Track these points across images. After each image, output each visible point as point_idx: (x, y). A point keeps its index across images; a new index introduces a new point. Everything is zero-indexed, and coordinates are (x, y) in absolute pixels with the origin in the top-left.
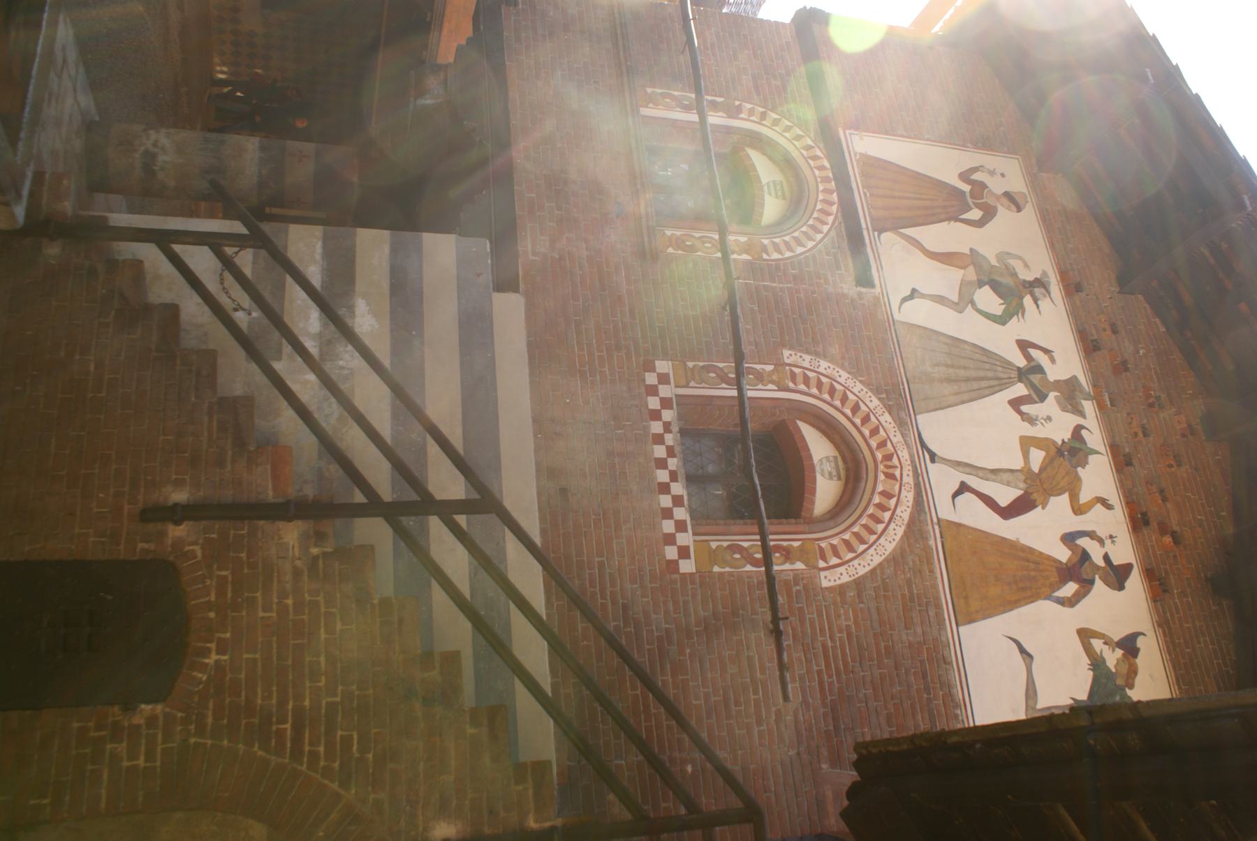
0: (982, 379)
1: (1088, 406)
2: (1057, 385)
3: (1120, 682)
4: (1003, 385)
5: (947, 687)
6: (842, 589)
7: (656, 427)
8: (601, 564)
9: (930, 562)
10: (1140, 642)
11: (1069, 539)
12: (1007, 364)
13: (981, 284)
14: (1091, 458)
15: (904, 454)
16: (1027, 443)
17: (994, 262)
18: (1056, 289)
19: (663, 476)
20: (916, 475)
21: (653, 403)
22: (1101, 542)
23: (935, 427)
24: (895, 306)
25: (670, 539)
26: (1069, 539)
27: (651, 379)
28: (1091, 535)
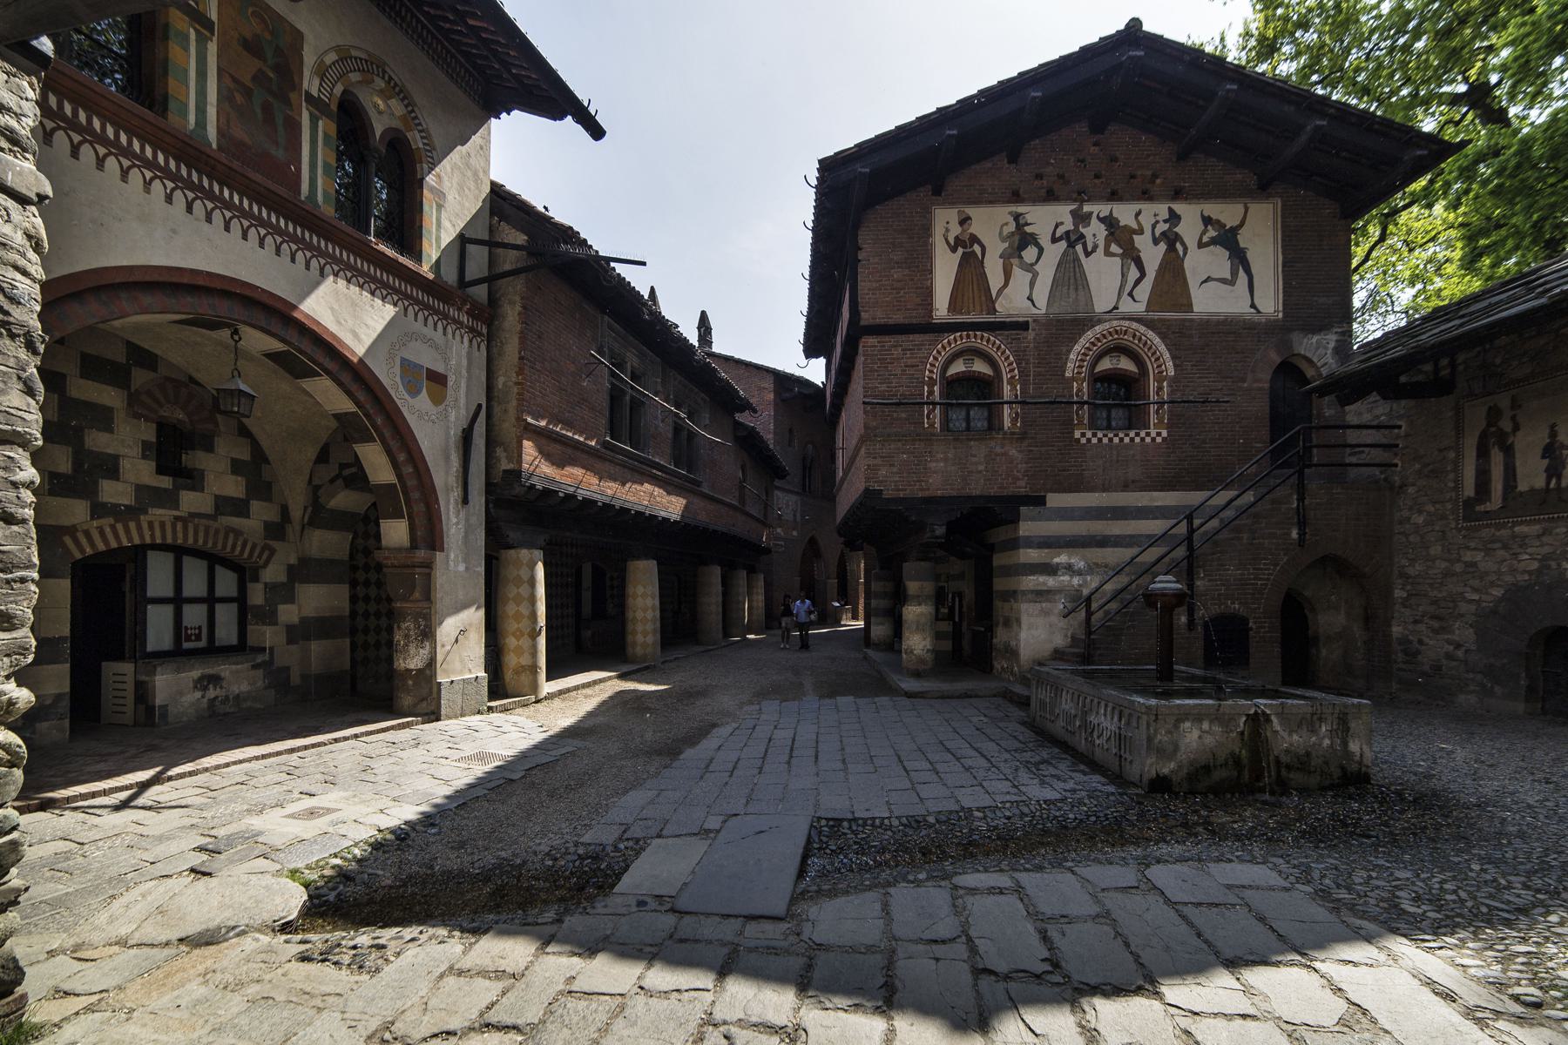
0: (1075, 271)
1: (1087, 208)
2: (1076, 225)
3: (1222, 231)
4: (1077, 259)
5: (1219, 323)
6: (1175, 365)
7: (1105, 440)
8: (1164, 469)
9: (1164, 320)
10: (1206, 214)
11: (1156, 241)
12: (1065, 254)
13: (1021, 257)
14: (1115, 215)
15: (1115, 323)
16: (1108, 253)
17: (1007, 245)
18: (1021, 209)
19: (1127, 440)
20: (1123, 319)
21: (1094, 441)
22: (1157, 222)
23: (1102, 303)
24: (1037, 312)
25: (1153, 440)
26: (1156, 241)
27: (1083, 441)
28: (1154, 227)
